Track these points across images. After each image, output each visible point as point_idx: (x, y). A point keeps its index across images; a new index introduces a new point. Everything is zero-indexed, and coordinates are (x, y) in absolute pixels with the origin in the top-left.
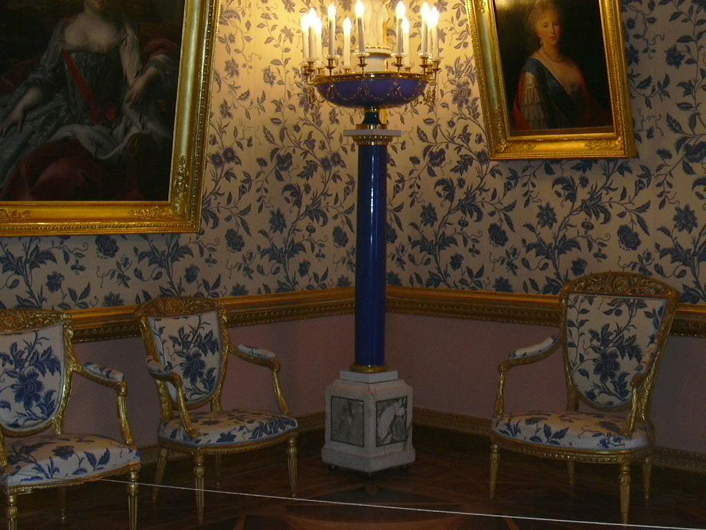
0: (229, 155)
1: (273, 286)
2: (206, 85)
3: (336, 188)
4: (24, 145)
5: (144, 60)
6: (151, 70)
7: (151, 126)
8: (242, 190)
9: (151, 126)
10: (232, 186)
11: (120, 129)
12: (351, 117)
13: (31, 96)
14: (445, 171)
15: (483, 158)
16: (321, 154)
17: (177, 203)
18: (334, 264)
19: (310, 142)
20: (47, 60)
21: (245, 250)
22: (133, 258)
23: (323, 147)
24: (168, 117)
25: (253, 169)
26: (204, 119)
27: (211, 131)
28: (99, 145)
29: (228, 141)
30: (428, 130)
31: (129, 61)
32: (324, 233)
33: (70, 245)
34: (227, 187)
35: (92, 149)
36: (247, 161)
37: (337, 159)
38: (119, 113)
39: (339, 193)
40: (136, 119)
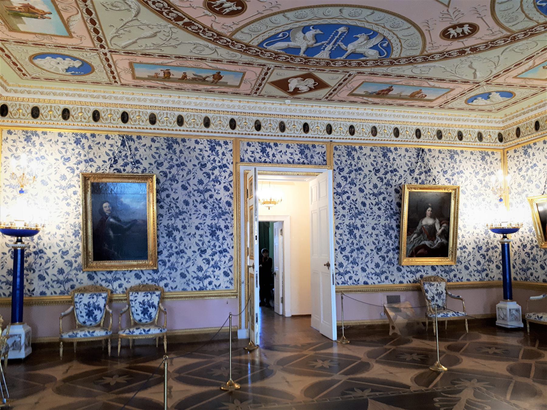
0: (464, 247)
1: (478, 279)
2: (457, 231)
3: (497, 254)
4: (414, 246)
5: (441, 226)
6: (443, 228)
7: (443, 240)
8: (468, 255)
9: (443, 240)
10: (466, 254)
11: (435, 242)
12: (499, 236)
13: (415, 236)
14: (482, 252)
15: (537, 246)
16: (491, 246)
17: (450, 257)
18: (496, 274)
19: (488, 243)
20: (418, 228)
21: (469, 270)
22: (440, 272)
23: (492, 244)
24: (447, 238)
25: (471, 250)
26: (456, 238)
27: (459, 241)
28: (431, 245)
29: (464, 244)
30: (522, 239)
31: (437, 227)
32: (493, 266)
33: (425, 268)
34: (463, 255)
35: (429, 246)
36: (470, 248)
37: (496, 247)
38: (435, 238)
39: (497, 256)
40: (439, 239)
